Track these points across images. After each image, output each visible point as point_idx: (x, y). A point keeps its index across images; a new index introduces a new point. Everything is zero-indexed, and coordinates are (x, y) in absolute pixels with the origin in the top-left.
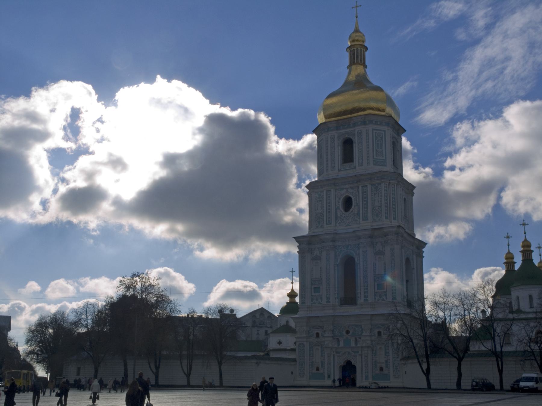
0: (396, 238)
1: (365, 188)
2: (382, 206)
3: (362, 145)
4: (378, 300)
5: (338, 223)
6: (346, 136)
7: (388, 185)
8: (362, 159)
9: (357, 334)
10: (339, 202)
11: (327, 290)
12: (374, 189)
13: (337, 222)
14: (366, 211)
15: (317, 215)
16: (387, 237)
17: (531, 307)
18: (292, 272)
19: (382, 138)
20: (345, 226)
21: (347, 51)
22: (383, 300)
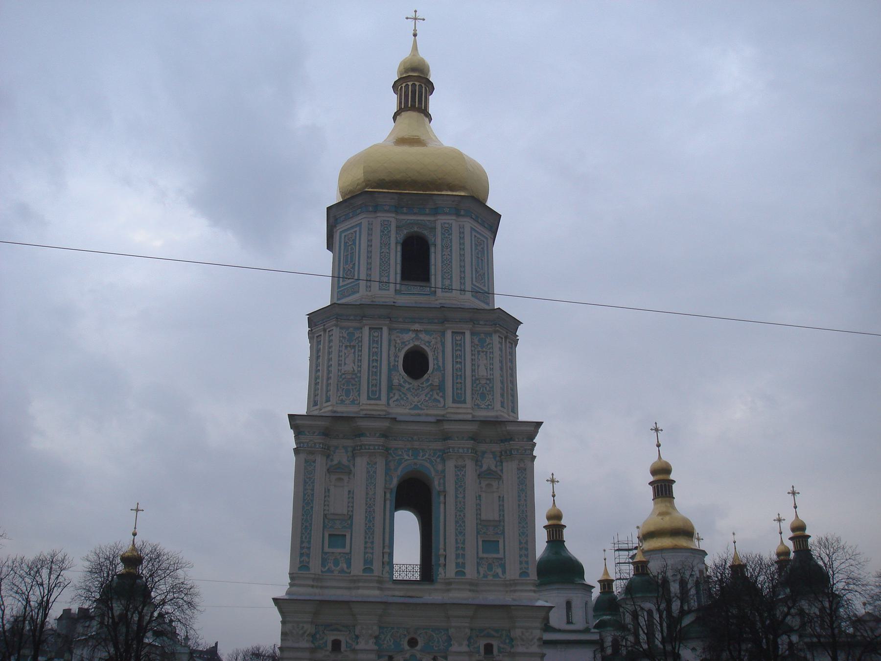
0: (530, 448)
1: (458, 338)
2: (493, 378)
3: (451, 253)
4: (485, 576)
5: (394, 401)
6: (416, 229)
7: (504, 340)
8: (451, 279)
9: (436, 649)
10: (396, 356)
11: (366, 543)
12: (477, 343)
13: (392, 398)
14: (460, 383)
15: (343, 376)
16: (511, 442)
17: (569, 622)
18: (137, 510)
19: (483, 248)
20: (410, 409)
21: (395, 87)
22: (496, 575)
